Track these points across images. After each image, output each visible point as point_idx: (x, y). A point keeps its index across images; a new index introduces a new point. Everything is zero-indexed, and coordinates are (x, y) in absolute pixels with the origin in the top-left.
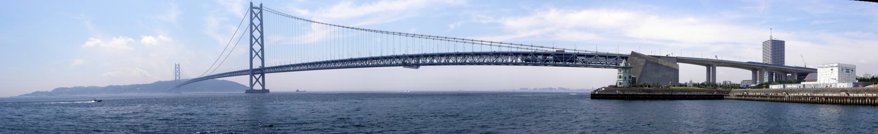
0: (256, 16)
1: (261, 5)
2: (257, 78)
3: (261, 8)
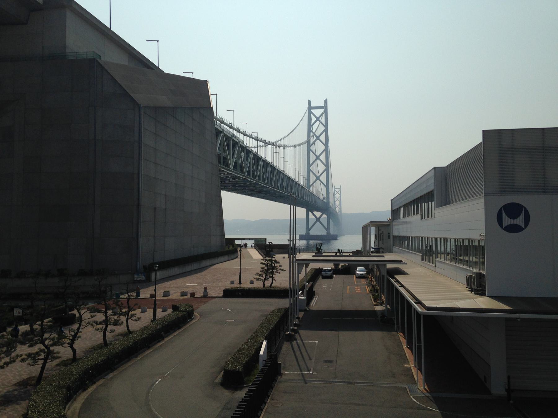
0: (318, 119)
1: (326, 101)
2: (318, 217)
3: (325, 108)
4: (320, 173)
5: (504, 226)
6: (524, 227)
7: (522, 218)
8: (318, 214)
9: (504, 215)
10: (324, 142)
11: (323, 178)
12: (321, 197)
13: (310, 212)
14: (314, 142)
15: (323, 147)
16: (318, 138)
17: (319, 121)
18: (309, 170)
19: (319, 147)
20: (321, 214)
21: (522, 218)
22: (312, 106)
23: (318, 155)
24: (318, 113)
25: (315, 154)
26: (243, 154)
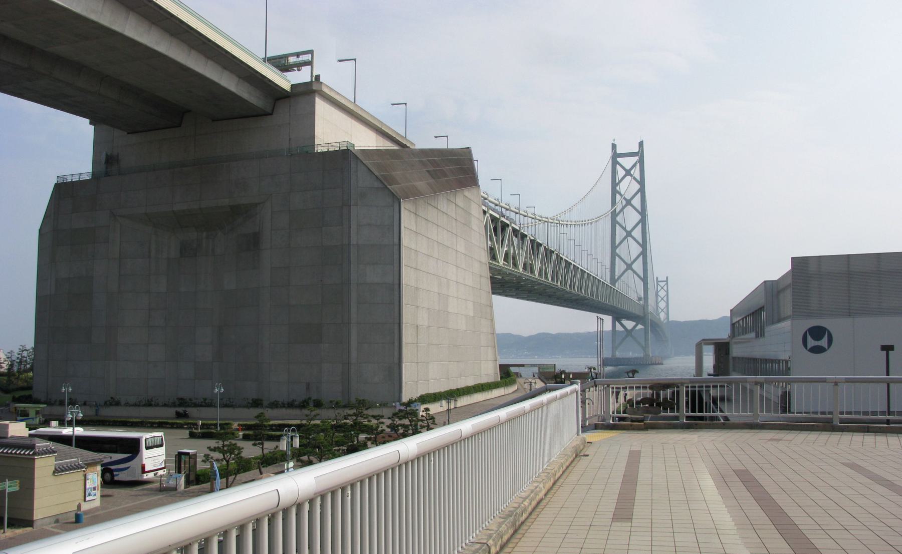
0: (628, 173)
1: (641, 144)
3: (640, 154)
4: (633, 259)
5: (809, 347)
6: (827, 348)
7: (826, 338)
8: (629, 324)
9: (809, 337)
10: (639, 208)
11: (638, 266)
12: (634, 297)
13: (617, 323)
14: (622, 210)
15: (638, 217)
16: (629, 202)
17: (631, 175)
18: (614, 255)
19: (630, 218)
20: (634, 323)
21: (826, 338)
22: (618, 152)
23: (629, 229)
24: (628, 162)
25: (624, 229)
26: (515, 240)
